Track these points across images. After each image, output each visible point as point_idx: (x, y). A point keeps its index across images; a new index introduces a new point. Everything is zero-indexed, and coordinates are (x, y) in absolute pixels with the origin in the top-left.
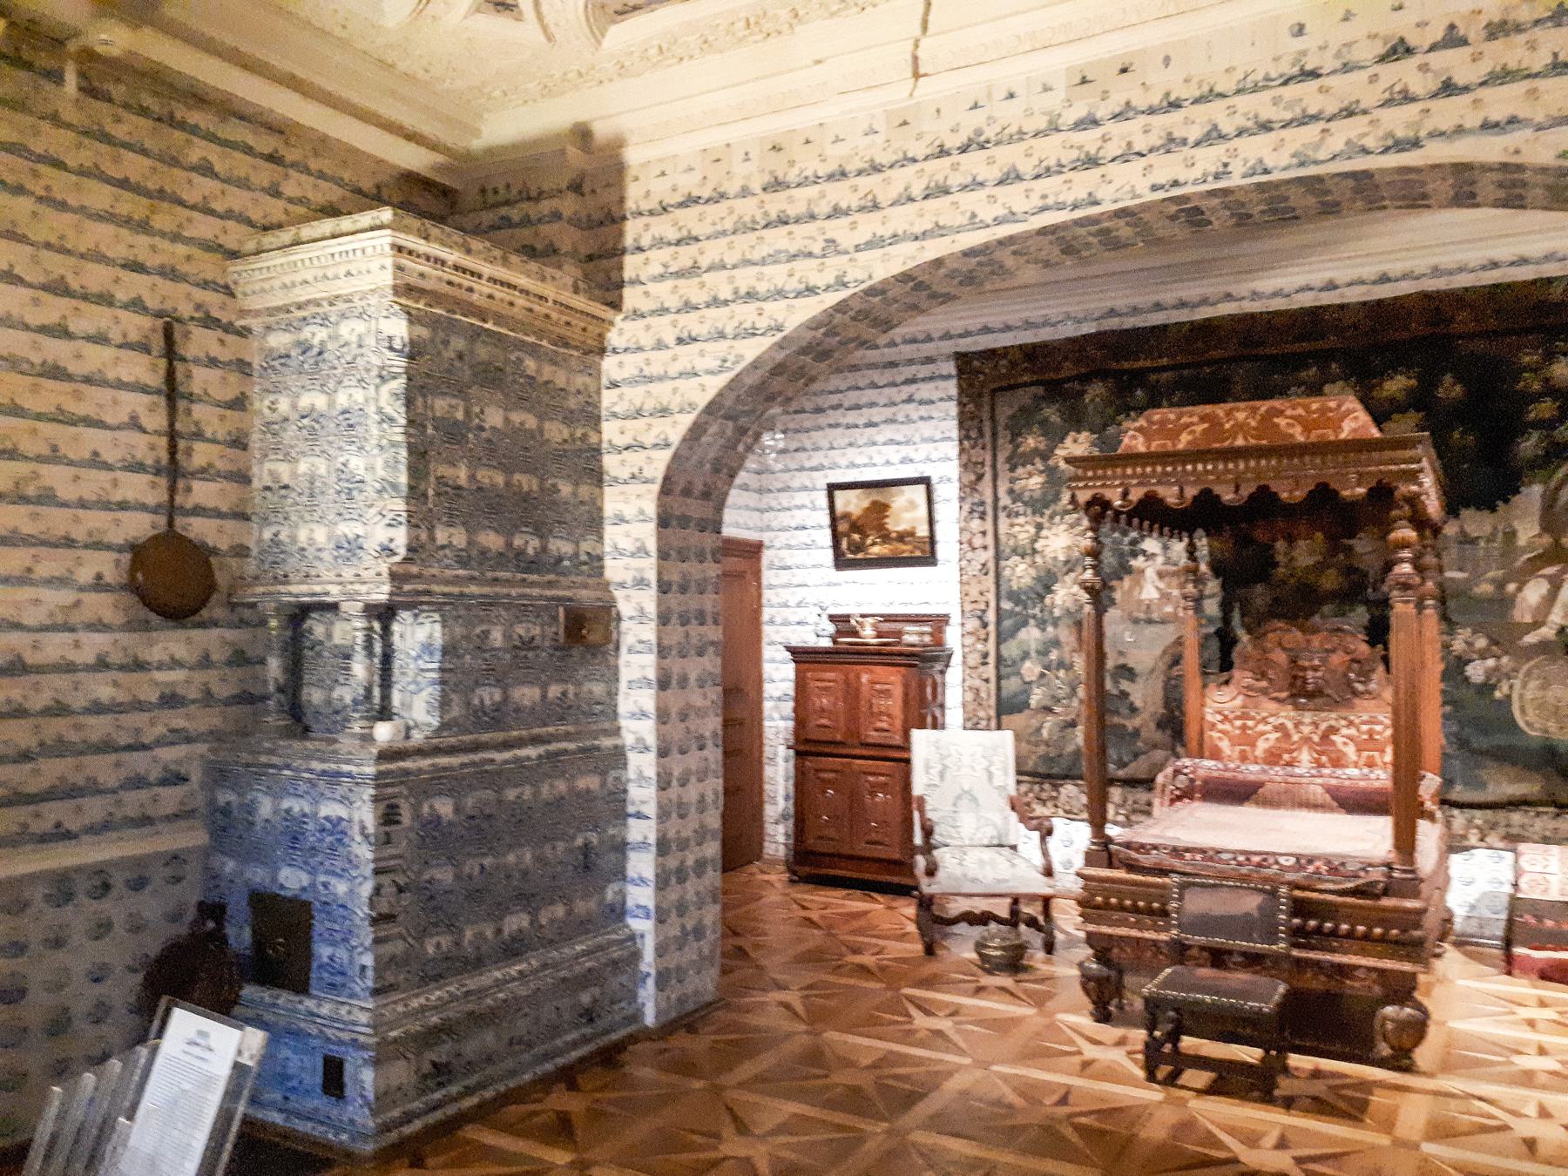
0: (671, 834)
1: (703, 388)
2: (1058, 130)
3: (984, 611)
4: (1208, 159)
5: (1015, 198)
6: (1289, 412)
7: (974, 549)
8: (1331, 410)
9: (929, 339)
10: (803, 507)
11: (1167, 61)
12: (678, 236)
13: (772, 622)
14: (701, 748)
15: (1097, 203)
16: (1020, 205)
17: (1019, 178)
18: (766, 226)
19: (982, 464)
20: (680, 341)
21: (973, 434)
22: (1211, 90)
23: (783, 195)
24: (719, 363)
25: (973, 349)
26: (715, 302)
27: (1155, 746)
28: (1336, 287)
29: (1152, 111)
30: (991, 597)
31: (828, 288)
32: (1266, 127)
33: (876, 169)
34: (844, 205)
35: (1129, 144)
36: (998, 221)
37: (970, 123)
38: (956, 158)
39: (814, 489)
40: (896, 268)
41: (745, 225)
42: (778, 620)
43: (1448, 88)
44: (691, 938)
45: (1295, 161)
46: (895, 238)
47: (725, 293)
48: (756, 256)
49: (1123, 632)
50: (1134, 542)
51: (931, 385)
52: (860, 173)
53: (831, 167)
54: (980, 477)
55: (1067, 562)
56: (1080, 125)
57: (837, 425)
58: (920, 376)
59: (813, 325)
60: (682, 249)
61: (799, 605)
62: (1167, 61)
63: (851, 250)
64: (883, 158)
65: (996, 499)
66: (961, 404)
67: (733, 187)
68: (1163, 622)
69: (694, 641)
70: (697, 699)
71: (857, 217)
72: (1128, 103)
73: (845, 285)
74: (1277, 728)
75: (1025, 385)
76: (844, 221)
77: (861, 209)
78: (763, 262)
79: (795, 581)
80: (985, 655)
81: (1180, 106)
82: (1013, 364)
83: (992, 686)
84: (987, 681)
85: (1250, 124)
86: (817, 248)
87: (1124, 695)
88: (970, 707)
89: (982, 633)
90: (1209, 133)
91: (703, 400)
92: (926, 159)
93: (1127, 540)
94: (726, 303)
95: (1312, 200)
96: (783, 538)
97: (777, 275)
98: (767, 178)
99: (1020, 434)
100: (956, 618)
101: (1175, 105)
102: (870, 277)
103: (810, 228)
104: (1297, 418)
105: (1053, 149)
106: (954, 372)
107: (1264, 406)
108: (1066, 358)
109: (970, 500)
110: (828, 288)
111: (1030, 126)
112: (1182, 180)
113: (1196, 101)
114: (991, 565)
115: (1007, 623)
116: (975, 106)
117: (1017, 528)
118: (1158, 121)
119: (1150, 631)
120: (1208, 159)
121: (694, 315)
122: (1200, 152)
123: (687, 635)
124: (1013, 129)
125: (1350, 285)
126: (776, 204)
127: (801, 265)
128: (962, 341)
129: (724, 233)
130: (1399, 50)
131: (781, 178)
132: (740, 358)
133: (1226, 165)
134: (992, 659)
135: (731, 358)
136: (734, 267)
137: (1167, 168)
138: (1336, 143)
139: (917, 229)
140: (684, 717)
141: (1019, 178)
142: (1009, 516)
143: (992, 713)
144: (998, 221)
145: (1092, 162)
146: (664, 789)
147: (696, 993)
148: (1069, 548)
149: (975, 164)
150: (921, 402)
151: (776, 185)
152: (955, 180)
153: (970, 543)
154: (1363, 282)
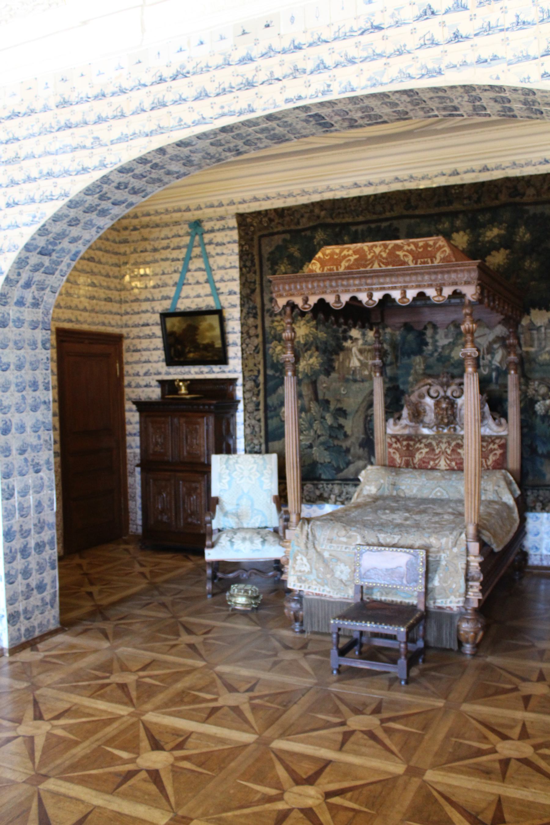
0: (16, 528)
1: (22, 235)
2: (229, 65)
3: (257, 377)
4: (318, 82)
5: (205, 108)
6: (406, 247)
7: (250, 337)
8: (430, 246)
9: (221, 205)
10: (147, 311)
11: (292, 19)
12: (7, 138)
13: (129, 385)
14: (37, 472)
15: (253, 111)
16: (208, 113)
17: (207, 95)
18: (58, 130)
19: (255, 283)
20: (8, 205)
21: (248, 264)
22: (319, 38)
23: (68, 109)
24: (31, 219)
25: (248, 211)
26: (29, 179)
27: (359, 458)
28: (458, 174)
29: (284, 52)
30: (261, 367)
31: (95, 168)
32: (352, 61)
34: (104, 115)
35: (272, 73)
36: (196, 123)
37: (178, 61)
38: (170, 83)
39: (153, 300)
40: (136, 154)
41: (46, 129)
42: (133, 384)
44: (35, 592)
45: (369, 83)
47: (34, 174)
48: (53, 149)
49: (339, 389)
50: (345, 331)
51: (223, 234)
52: (113, 94)
53: (96, 91)
54: (253, 291)
55: (305, 345)
56: (243, 61)
57: (166, 259)
58: (216, 228)
59: (88, 191)
60: (10, 146)
61: (146, 374)
62: (292, 19)
63: (109, 143)
64: (126, 85)
65: (263, 305)
66: (241, 245)
67: (38, 106)
68: (363, 381)
69: (30, 401)
70: (32, 440)
71: (112, 122)
72: (270, 48)
73: (105, 166)
74: (426, 446)
75: (278, 233)
76: (105, 125)
77: (114, 117)
78: (56, 153)
79: (143, 359)
80: (258, 404)
81: (300, 49)
82: (271, 220)
83: (262, 424)
84: (259, 421)
85: (342, 60)
87: (341, 427)
88: (249, 438)
89: (256, 390)
90: (318, 66)
91: (22, 243)
92: (152, 84)
93: (341, 330)
94: (35, 179)
95: (387, 110)
96: (135, 331)
97: (65, 161)
98: (59, 99)
99: (277, 264)
100: (240, 382)
101: (298, 48)
102: (120, 161)
103: (84, 130)
104: (410, 252)
105: (226, 77)
106: (236, 225)
107: (391, 243)
108: (302, 216)
109: (247, 306)
110: (95, 168)
111: (213, 63)
112: (303, 96)
113: (310, 45)
114: (261, 347)
115: (271, 384)
116: (181, 50)
117: (276, 324)
118: (289, 58)
119: (355, 387)
121: (17, 188)
122: (314, 78)
123: (24, 398)
124: (203, 65)
125: (466, 172)
126: (64, 115)
127: (80, 153)
128: (241, 206)
129: (33, 135)
131: (67, 99)
132: (43, 214)
133: (329, 86)
134: (262, 407)
135: (38, 215)
136: (40, 156)
138: (393, 72)
139: (147, 130)
140: (22, 451)
141: (207, 95)
142: (271, 316)
143: (262, 441)
144: (196, 123)
145: (250, 85)
146: (8, 499)
147: (40, 625)
148: (307, 335)
149: (181, 87)
150: (217, 244)
151: (64, 103)
152: (170, 97)
153: (248, 333)
154: (473, 171)
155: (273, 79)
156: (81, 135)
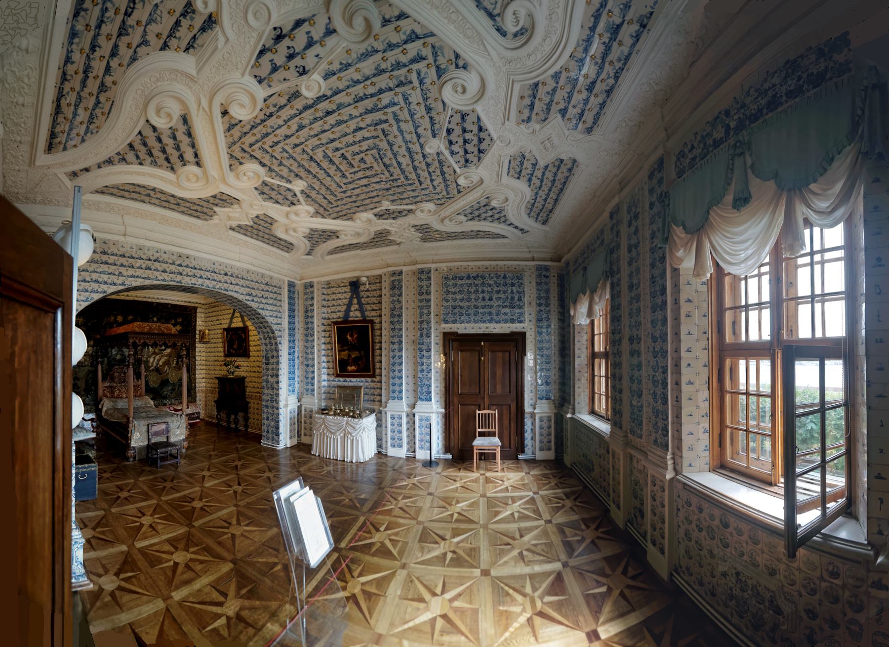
5: (165, 276)
16: (167, 279)
33: (133, 258)
43: (231, 283)
46: (138, 277)
47: (88, 279)
86: (117, 273)
97: (105, 277)
105: (173, 268)
120: (200, 281)
130: (226, 274)
132: (92, 298)
137: (194, 281)
138: (218, 286)
145: (181, 274)
152: (153, 267)
155: (187, 275)
156: (112, 268)
